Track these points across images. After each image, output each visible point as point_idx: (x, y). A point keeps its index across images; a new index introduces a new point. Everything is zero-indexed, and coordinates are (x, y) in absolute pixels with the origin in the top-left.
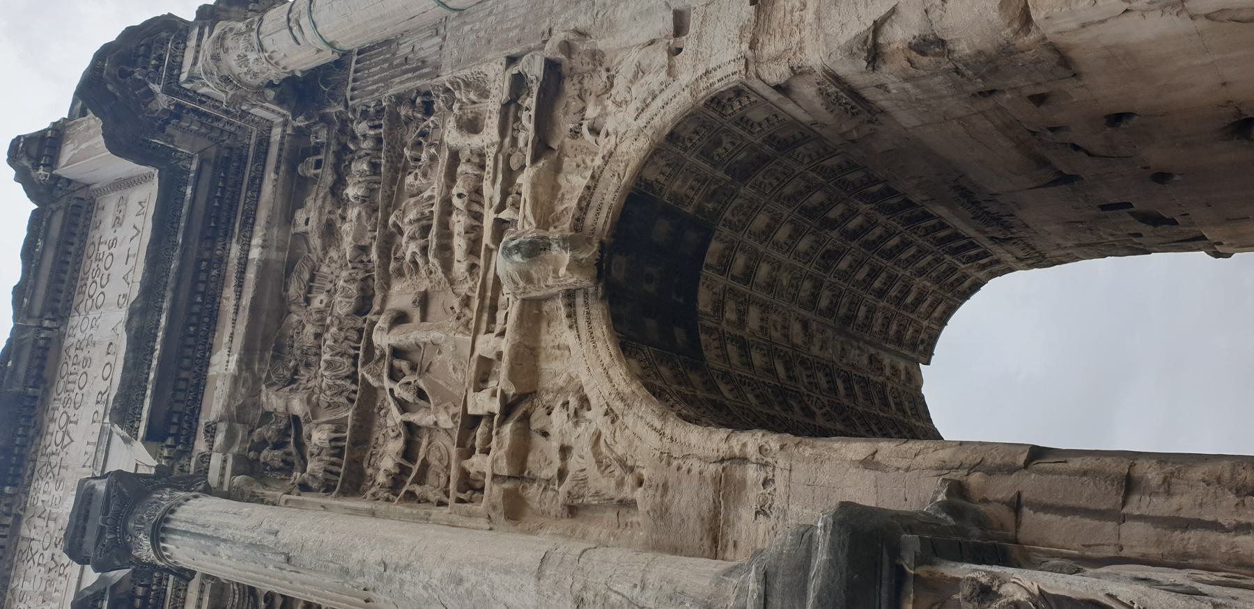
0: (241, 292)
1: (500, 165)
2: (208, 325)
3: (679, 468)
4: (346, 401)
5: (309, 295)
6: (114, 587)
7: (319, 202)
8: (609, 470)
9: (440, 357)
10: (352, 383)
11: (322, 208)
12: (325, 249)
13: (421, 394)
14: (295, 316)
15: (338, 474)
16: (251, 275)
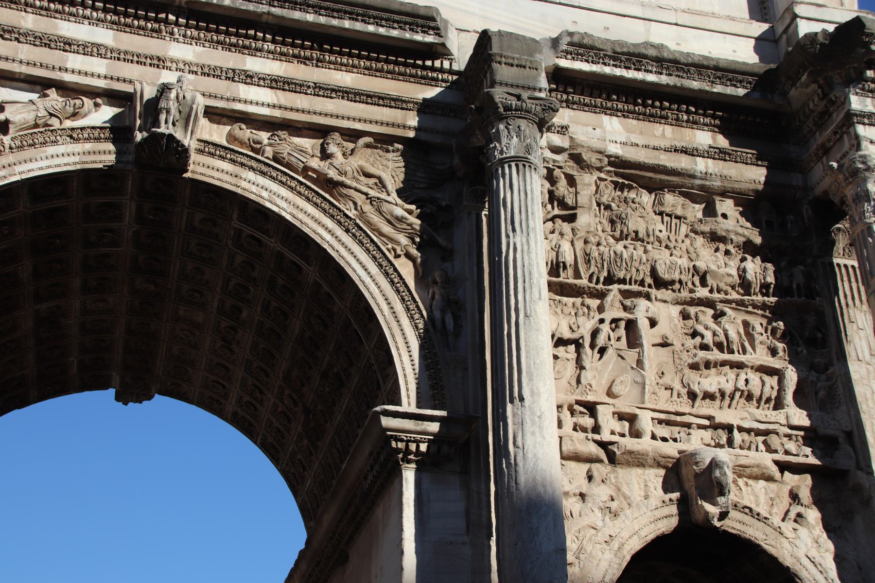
0: (671, 151)
1: (771, 427)
4: (591, 272)
5: (664, 215)
6: (443, 45)
7: (740, 230)
8: (576, 539)
10: (605, 277)
11: (737, 234)
13: (602, 351)
14: (647, 199)
16: (682, 162)
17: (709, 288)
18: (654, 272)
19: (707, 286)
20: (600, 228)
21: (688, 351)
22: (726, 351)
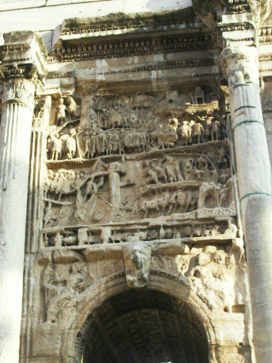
0: (135, 71)
1: (186, 222)
2: (120, 53)
3: (58, 339)
4: (86, 152)
9: (104, 203)
12: (158, 114)
13: (89, 196)
15: (54, 159)
17: (159, 146)
18: (123, 144)
19: (159, 145)
20: (94, 125)
21: (143, 186)
22: (167, 182)
